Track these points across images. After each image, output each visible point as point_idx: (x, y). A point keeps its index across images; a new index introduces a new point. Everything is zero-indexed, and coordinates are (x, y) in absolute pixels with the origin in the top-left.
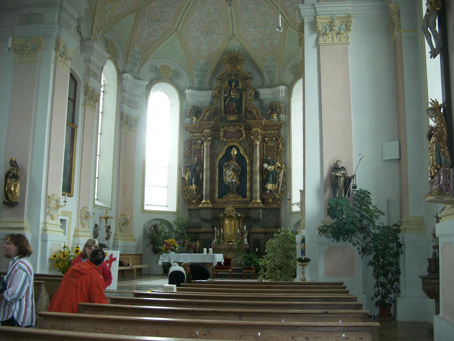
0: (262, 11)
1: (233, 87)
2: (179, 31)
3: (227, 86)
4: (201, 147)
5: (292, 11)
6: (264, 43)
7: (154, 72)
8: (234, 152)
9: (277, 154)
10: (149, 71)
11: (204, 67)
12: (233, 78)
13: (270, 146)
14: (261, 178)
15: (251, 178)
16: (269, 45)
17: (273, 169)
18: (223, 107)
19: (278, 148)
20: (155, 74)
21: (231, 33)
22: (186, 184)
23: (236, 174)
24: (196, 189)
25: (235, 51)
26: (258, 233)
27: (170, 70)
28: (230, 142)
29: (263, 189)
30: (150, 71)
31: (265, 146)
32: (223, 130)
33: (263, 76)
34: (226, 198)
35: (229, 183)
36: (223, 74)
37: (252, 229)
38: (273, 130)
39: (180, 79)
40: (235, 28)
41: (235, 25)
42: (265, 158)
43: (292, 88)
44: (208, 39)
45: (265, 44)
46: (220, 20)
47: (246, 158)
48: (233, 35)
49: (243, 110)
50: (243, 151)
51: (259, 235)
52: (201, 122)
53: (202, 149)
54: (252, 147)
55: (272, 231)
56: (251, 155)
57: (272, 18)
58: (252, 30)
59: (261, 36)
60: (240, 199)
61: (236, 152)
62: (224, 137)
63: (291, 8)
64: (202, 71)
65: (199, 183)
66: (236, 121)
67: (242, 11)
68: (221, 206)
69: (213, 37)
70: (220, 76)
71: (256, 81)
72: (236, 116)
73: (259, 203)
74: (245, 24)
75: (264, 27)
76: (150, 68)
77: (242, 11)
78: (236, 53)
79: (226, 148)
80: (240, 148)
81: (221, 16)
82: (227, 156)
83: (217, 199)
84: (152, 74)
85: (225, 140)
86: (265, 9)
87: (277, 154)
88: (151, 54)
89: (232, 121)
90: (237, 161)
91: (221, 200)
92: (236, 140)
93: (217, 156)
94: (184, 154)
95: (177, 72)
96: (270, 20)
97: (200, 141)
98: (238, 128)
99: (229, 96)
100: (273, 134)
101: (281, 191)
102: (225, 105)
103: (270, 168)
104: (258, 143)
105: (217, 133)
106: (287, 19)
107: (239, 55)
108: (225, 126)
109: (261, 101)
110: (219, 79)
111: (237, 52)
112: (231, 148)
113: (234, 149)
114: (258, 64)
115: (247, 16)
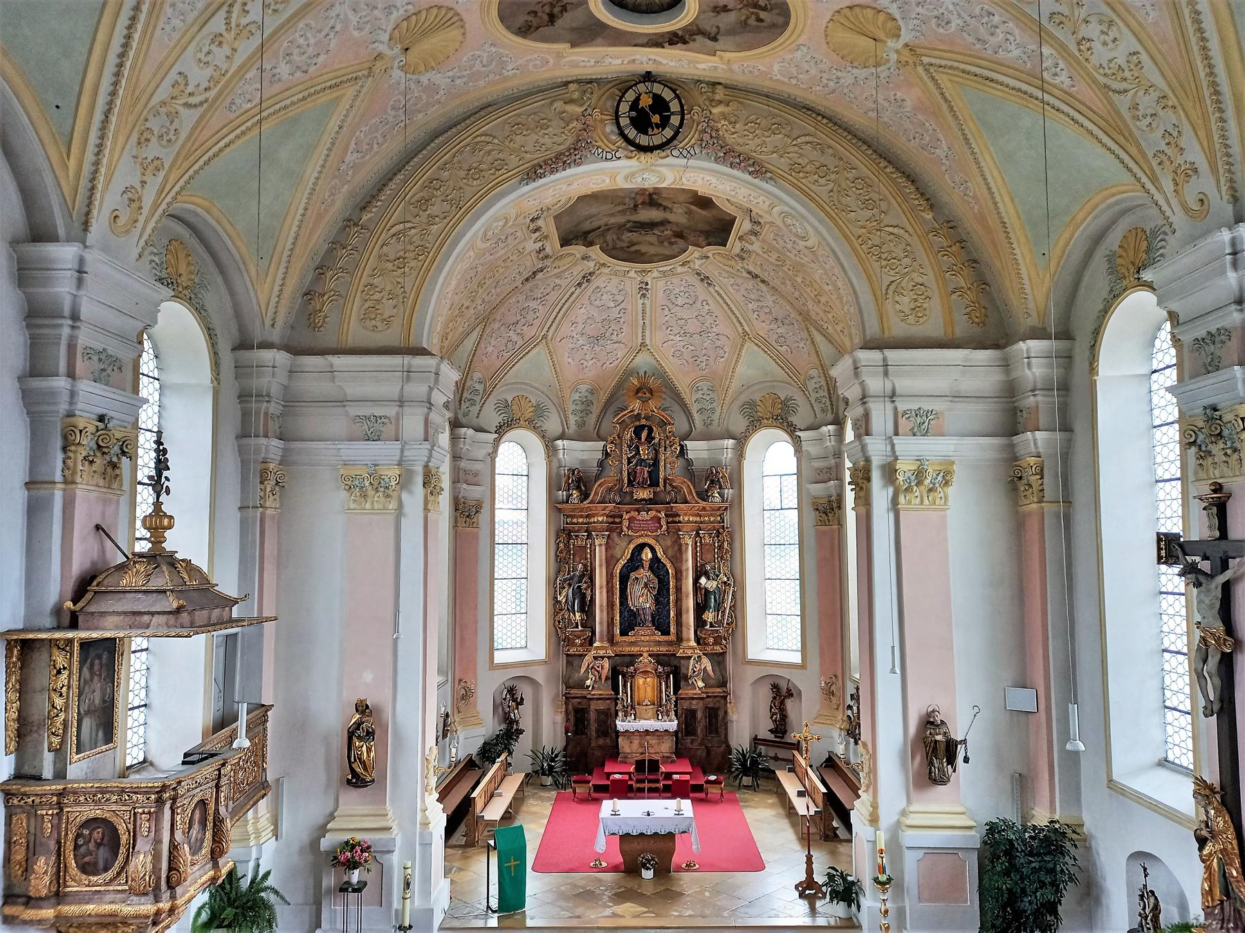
12: (643, 422)
13: (706, 544)
15: (678, 601)
17: (714, 586)
18: (625, 474)
19: (720, 547)
21: (640, 340)
22: (561, 610)
24: (582, 620)
28: (640, 536)
29: (700, 623)
47: (668, 565)
48: (643, 344)
51: (694, 702)
54: (680, 550)
56: (677, 559)
60: (659, 637)
61: (650, 556)
65: (587, 607)
68: (627, 650)
71: (680, 425)
79: (632, 546)
80: (658, 548)
82: (634, 563)
89: (644, 500)
91: (624, 638)
99: (636, 454)
100: (712, 522)
103: (711, 585)
104: (690, 542)
105: (617, 520)
108: (631, 509)
109: (689, 462)
112: (641, 547)
114: (684, 396)
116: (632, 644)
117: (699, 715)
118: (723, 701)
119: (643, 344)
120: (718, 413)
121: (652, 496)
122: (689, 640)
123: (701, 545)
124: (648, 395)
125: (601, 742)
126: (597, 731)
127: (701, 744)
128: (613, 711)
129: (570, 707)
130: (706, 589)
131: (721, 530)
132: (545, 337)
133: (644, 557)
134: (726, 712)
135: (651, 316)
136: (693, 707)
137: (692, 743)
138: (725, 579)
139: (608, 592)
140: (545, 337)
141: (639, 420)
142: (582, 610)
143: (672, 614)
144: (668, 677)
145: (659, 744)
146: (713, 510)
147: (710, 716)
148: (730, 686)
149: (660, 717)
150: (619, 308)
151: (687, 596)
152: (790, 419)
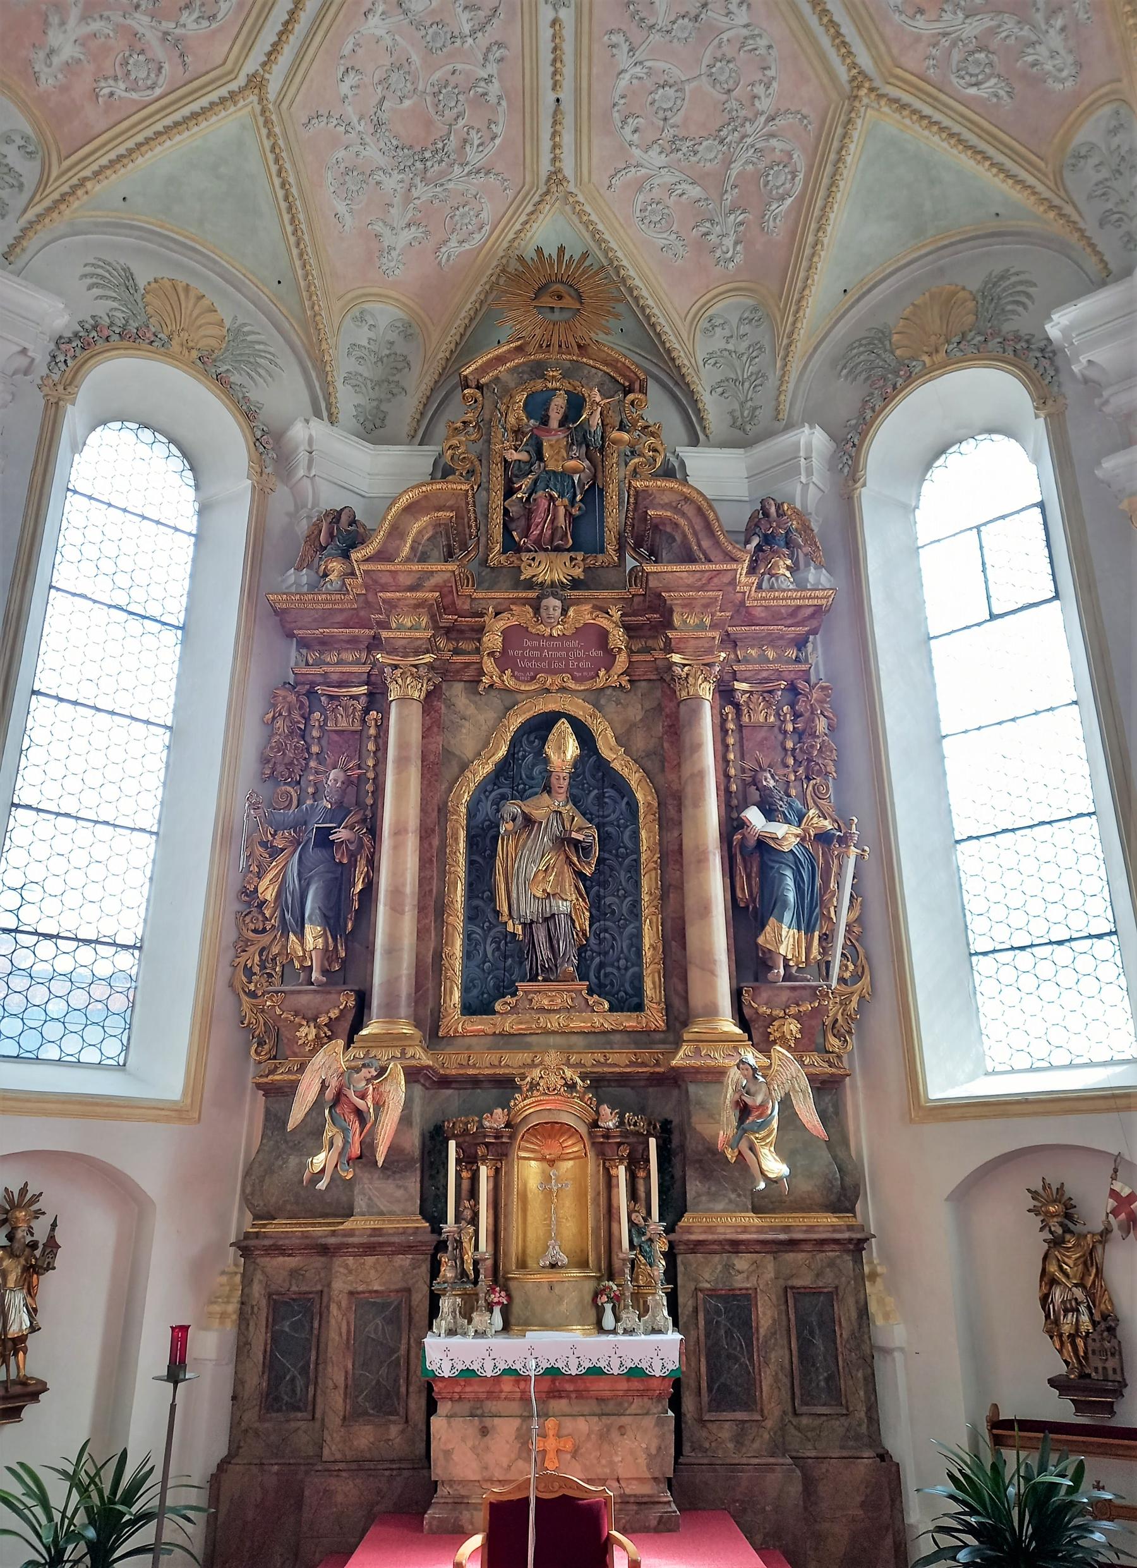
0: (725, 36)
1: (554, 423)
2: (271, 96)
3: (519, 419)
4: (364, 721)
6: (707, 234)
7: (114, 295)
8: (561, 749)
9: (801, 770)
11: (392, 343)
13: (756, 727)
14: (729, 897)
16: (736, 243)
18: (498, 518)
20: (115, 305)
21: (545, 166)
23: (580, 875)
24: (328, 955)
25: (567, 257)
26: (735, 1246)
27: (211, 317)
30: (89, 281)
31: (731, 726)
32: (501, 624)
34: (514, 1009)
35: (528, 926)
36: (500, 360)
37: (686, 1220)
38: (773, 641)
39: (260, 375)
40: (567, 138)
41: (568, 120)
42: (734, 787)
43: (862, 442)
44: (422, 192)
45: (713, 238)
46: (495, 88)
47: (634, 777)
48: (556, 178)
50: (613, 741)
51: (742, 1262)
53: (372, 731)
55: (811, 1229)
57: (770, 73)
58: (655, 158)
59: (695, 192)
60: (602, 1017)
61: (572, 748)
62: (504, 661)
64: (381, 360)
66: (576, 584)
67: (614, 39)
68: (485, 1063)
69: (451, 185)
70: (483, 370)
72: (572, 559)
73: (726, 1039)
74: (624, 122)
75: (721, 142)
76: (93, 265)
77: (614, 39)
79: (515, 722)
81: (501, 60)
83: (456, 1014)
84: (101, 297)
85: (510, 683)
87: (801, 770)
88: (96, 174)
90: (575, 800)
91: (479, 1024)
92: (572, 685)
93: (464, 766)
94: (265, 760)
95: (249, 338)
96: (759, 90)
97: (363, 689)
98: (582, 614)
101: (842, 980)
102: (506, 512)
103: (785, 834)
104: (706, 691)
106: (864, 60)
108: (515, 601)
110: (479, 387)
111: (576, 257)
112: (542, 725)
113: (564, 725)
114: (672, 341)
115: (638, 69)
116: (506, 1040)
117: (765, 1315)
118: (848, 1261)
120: (772, 381)
122: (712, 1012)
123: (740, 727)
124: (569, 302)
125: (365, 1437)
126: (352, 1390)
127: (778, 1447)
128: (420, 1298)
129: (257, 1289)
130: (764, 846)
131: (801, 685)
133: (550, 750)
134: (864, 1312)
135: (577, 77)
136: (739, 1282)
137: (739, 1440)
138: (827, 824)
139: (425, 862)
141: (543, 376)
142: (332, 922)
143: (649, 937)
144: (636, 1163)
145: (604, 1436)
146: (775, 617)
147: (802, 1322)
148: (869, 1212)
149: (609, 1321)
150: (483, 40)
151: (702, 860)
152: (1007, 328)
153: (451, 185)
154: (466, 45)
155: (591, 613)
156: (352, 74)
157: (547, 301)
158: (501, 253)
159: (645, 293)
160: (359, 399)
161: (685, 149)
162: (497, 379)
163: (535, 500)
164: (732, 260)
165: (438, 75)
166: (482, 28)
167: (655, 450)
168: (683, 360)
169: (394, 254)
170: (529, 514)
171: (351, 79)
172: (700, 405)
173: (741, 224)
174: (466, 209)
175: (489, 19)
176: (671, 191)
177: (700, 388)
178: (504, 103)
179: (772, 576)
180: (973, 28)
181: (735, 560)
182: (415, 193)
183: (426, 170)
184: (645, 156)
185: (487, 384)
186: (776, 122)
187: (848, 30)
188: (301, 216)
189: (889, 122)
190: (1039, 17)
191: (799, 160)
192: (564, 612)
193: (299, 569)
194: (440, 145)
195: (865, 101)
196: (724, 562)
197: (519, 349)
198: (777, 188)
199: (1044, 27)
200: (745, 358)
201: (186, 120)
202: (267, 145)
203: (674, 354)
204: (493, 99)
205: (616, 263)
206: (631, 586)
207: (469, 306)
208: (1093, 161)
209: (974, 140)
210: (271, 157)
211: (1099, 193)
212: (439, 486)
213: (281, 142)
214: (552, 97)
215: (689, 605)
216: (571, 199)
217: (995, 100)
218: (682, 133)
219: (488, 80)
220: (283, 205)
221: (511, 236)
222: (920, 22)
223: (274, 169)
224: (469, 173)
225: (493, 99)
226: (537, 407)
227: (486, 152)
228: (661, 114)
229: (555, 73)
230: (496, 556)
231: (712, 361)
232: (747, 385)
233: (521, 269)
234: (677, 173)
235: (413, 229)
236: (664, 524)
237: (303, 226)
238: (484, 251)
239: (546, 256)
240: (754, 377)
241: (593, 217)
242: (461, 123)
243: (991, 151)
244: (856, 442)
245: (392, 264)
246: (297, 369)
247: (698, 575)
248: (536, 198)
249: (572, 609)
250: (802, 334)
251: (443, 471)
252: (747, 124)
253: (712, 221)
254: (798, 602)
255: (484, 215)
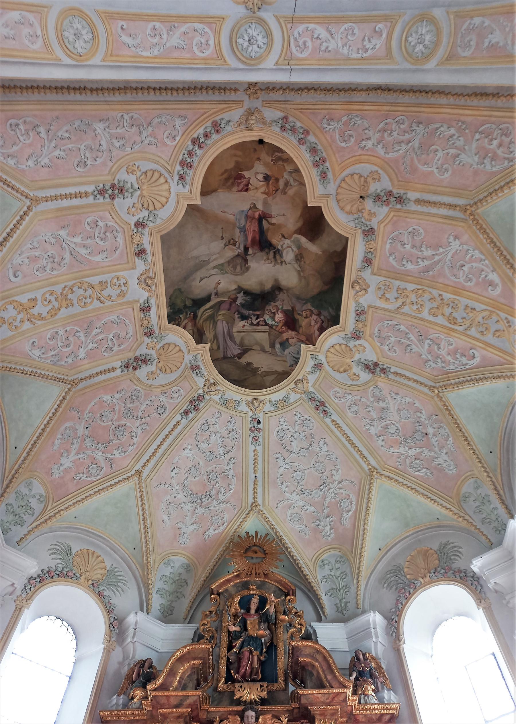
0: (319, 455)
1: (253, 611)
2: (143, 478)
3: (236, 610)
5: (383, 443)
6: (318, 525)
10: (50, 549)
16: (331, 529)
18: (224, 663)
21: (251, 500)
25: (259, 536)
33: (318, 600)
36: (228, 581)
40: (259, 490)
44: (200, 511)
45: (320, 527)
46: (231, 473)
48: (255, 504)
49: (280, 673)
52: (161, 694)
58: (295, 496)
59: (312, 509)
63: (381, 438)
66: (263, 701)
67: (277, 456)
69: (211, 508)
70: (220, 586)
72: (261, 686)
74: (282, 484)
75: (321, 490)
77: (277, 456)
78: (260, 539)
86: (325, 448)
88: (66, 508)
96: (334, 472)
102: (228, 659)
106: (373, 462)
107: (266, 542)
108: (231, 713)
110: (219, 594)
111: (263, 536)
114: (306, 571)
115: (287, 465)
119: (255, 504)
120: (353, 590)
121: (264, 694)
132: (138, 473)
135: (263, 468)
140: (138, 473)
141: (248, 589)
150: (227, 457)
153: (211, 508)
154: (221, 459)
155: (271, 720)
156: (176, 469)
157: (250, 554)
158: (231, 534)
159: (293, 550)
160: (163, 601)
161: (306, 493)
162: (226, 590)
163: (243, 652)
164: (329, 536)
165: (209, 469)
166: (228, 453)
167: (301, 625)
168: (311, 580)
169: (185, 535)
170: (239, 660)
171: (176, 470)
172: (321, 601)
173: (332, 521)
174: (218, 517)
175: (230, 450)
176: (302, 509)
177: (320, 593)
178: (235, 478)
179: (366, 695)
180: (412, 453)
181: (345, 687)
182: (197, 511)
183: (202, 502)
184: (291, 496)
185: (222, 593)
186: (342, 483)
187: (365, 453)
188: (148, 522)
189: (387, 484)
190: (437, 449)
191: (353, 497)
192: (257, 719)
193: (119, 695)
194: (208, 493)
195: (376, 476)
196: (338, 688)
197: (237, 576)
198: (345, 508)
199: (439, 453)
200: (339, 579)
201: (107, 487)
202: (139, 495)
203: (308, 577)
204: (231, 477)
205: (280, 538)
206: (292, 702)
207: (216, 557)
208: (472, 499)
209: (422, 491)
210: (139, 499)
211: (478, 511)
212: (195, 646)
213: (144, 494)
214: (254, 475)
215: (323, 714)
216: (261, 513)
217: (426, 476)
218: (305, 487)
219: (229, 470)
220: (141, 518)
221: (236, 527)
222: (392, 450)
223: (140, 504)
224: (220, 503)
225: (231, 477)
226: (245, 604)
227: (227, 495)
228: (296, 481)
229: (255, 467)
230: (222, 685)
231: (325, 580)
232: (342, 591)
233: (239, 541)
234: (304, 502)
235: (195, 525)
236: (308, 666)
237: (148, 526)
238: (224, 533)
239: (250, 535)
240: (344, 588)
241: (270, 519)
242: (217, 485)
243: (430, 495)
244: (397, 620)
245: (184, 540)
246: (135, 587)
247: (326, 696)
248: (247, 512)
249: (261, 717)
250: (363, 568)
251: (198, 637)
252: (331, 484)
253: (320, 520)
254: (381, 712)
255: (225, 519)
